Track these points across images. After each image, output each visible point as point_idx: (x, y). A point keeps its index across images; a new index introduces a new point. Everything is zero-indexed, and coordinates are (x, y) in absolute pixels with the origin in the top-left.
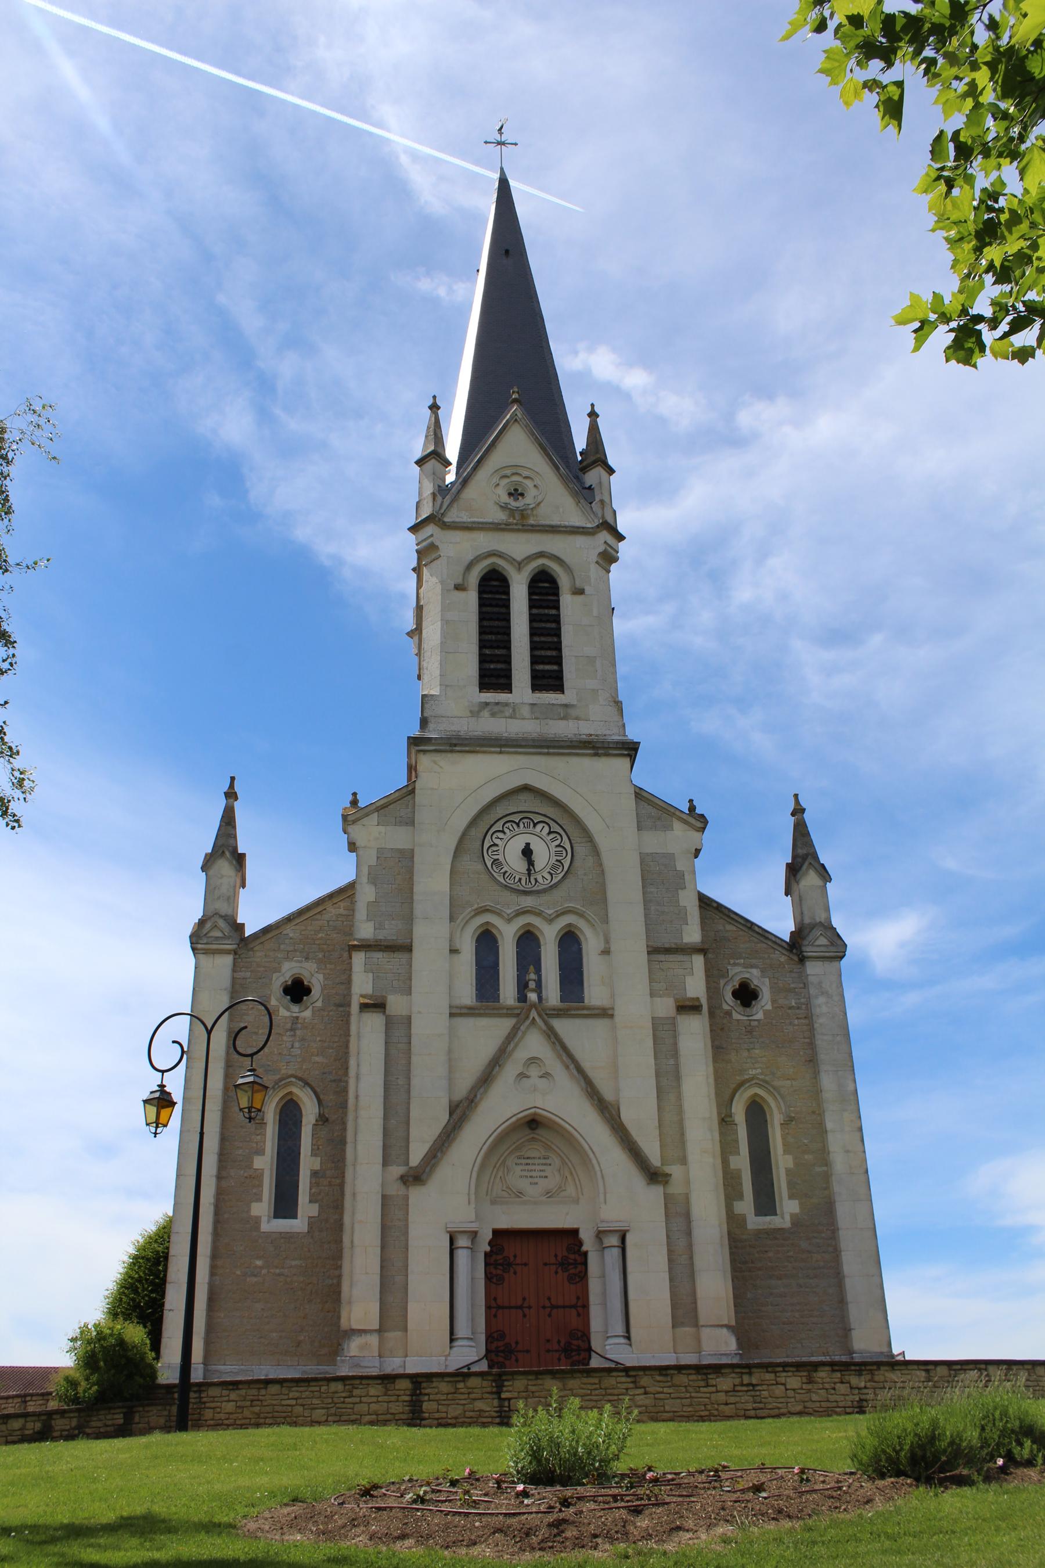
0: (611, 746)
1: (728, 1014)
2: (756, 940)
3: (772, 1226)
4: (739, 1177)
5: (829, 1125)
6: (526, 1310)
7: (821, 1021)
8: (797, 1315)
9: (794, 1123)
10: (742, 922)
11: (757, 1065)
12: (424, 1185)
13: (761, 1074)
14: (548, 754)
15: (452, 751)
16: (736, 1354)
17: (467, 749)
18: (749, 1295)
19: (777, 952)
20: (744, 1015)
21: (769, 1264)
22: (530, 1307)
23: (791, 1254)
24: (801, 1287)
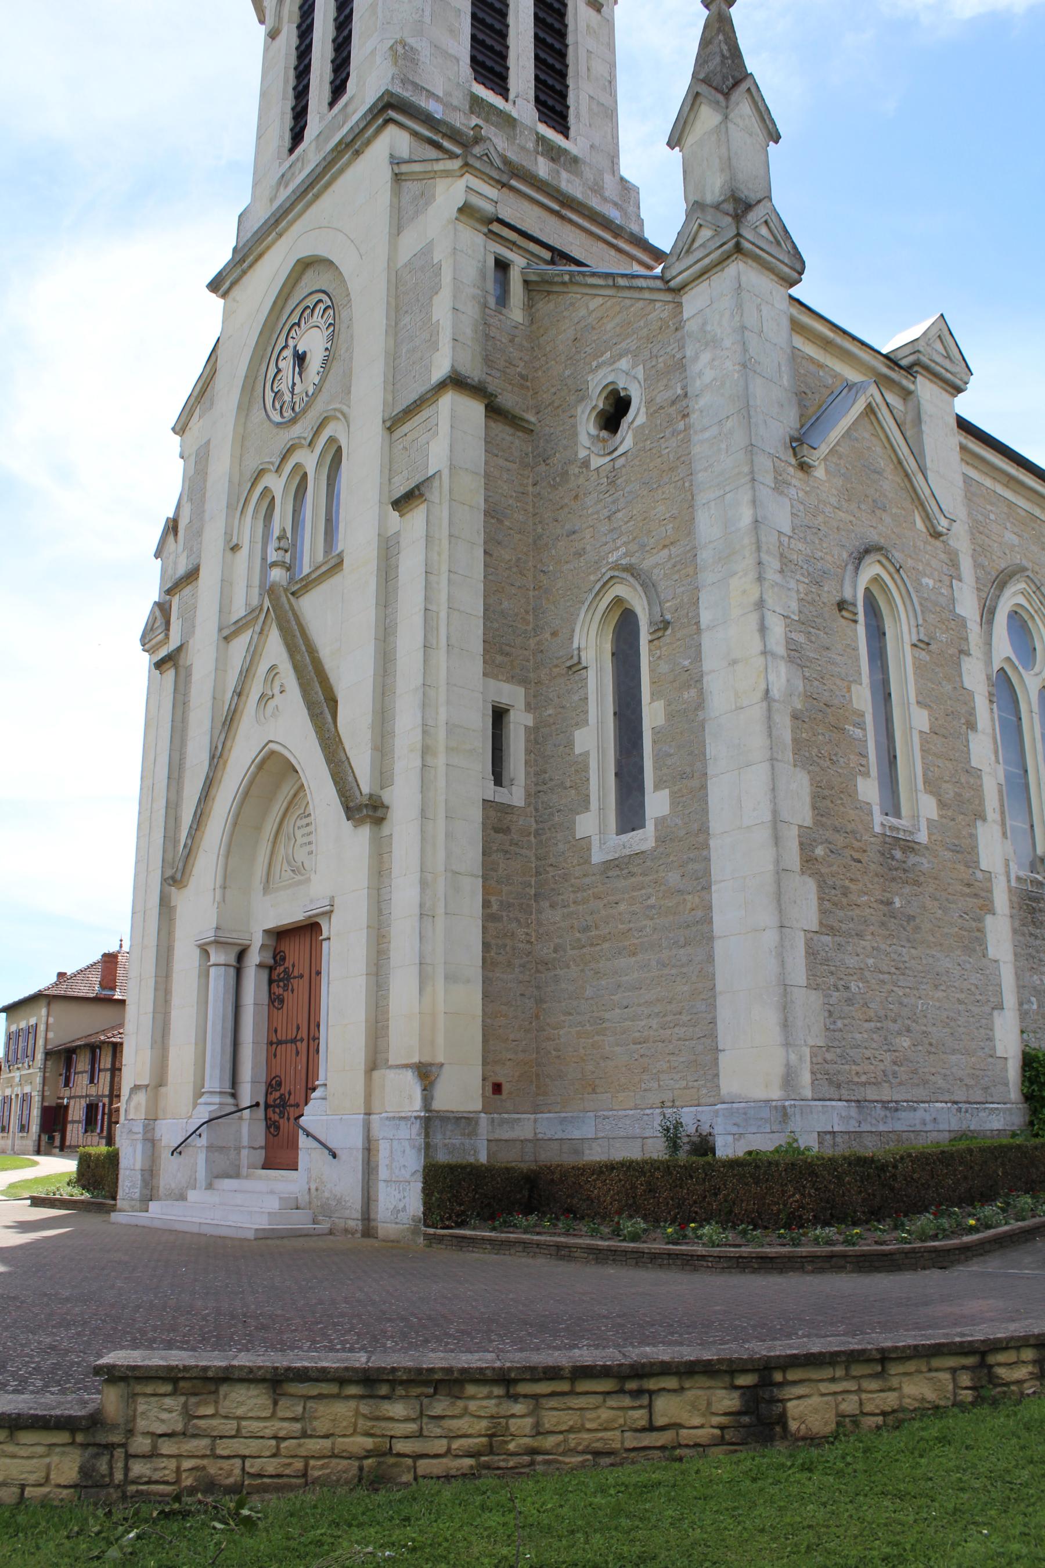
0: (361, 126)
1: (586, 464)
2: (628, 302)
3: (627, 852)
4: (586, 768)
5: (706, 617)
6: (299, 1043)
7: (702, 402)
8: (654, 1023)
9: (669, 632)
10: (600, 282)
11: (619, 542)
12: (185, 886)
13: (626, 555)
14: (317, 197)
15: (244, 272)
16: (416, 1118)
17: (251, 258)
18: (589, 992)
19: (658, 305)
20: (604, 455)
21: (620, 926)
22: (302, 1040)
23: (652, 901)
24: (664, 966)
